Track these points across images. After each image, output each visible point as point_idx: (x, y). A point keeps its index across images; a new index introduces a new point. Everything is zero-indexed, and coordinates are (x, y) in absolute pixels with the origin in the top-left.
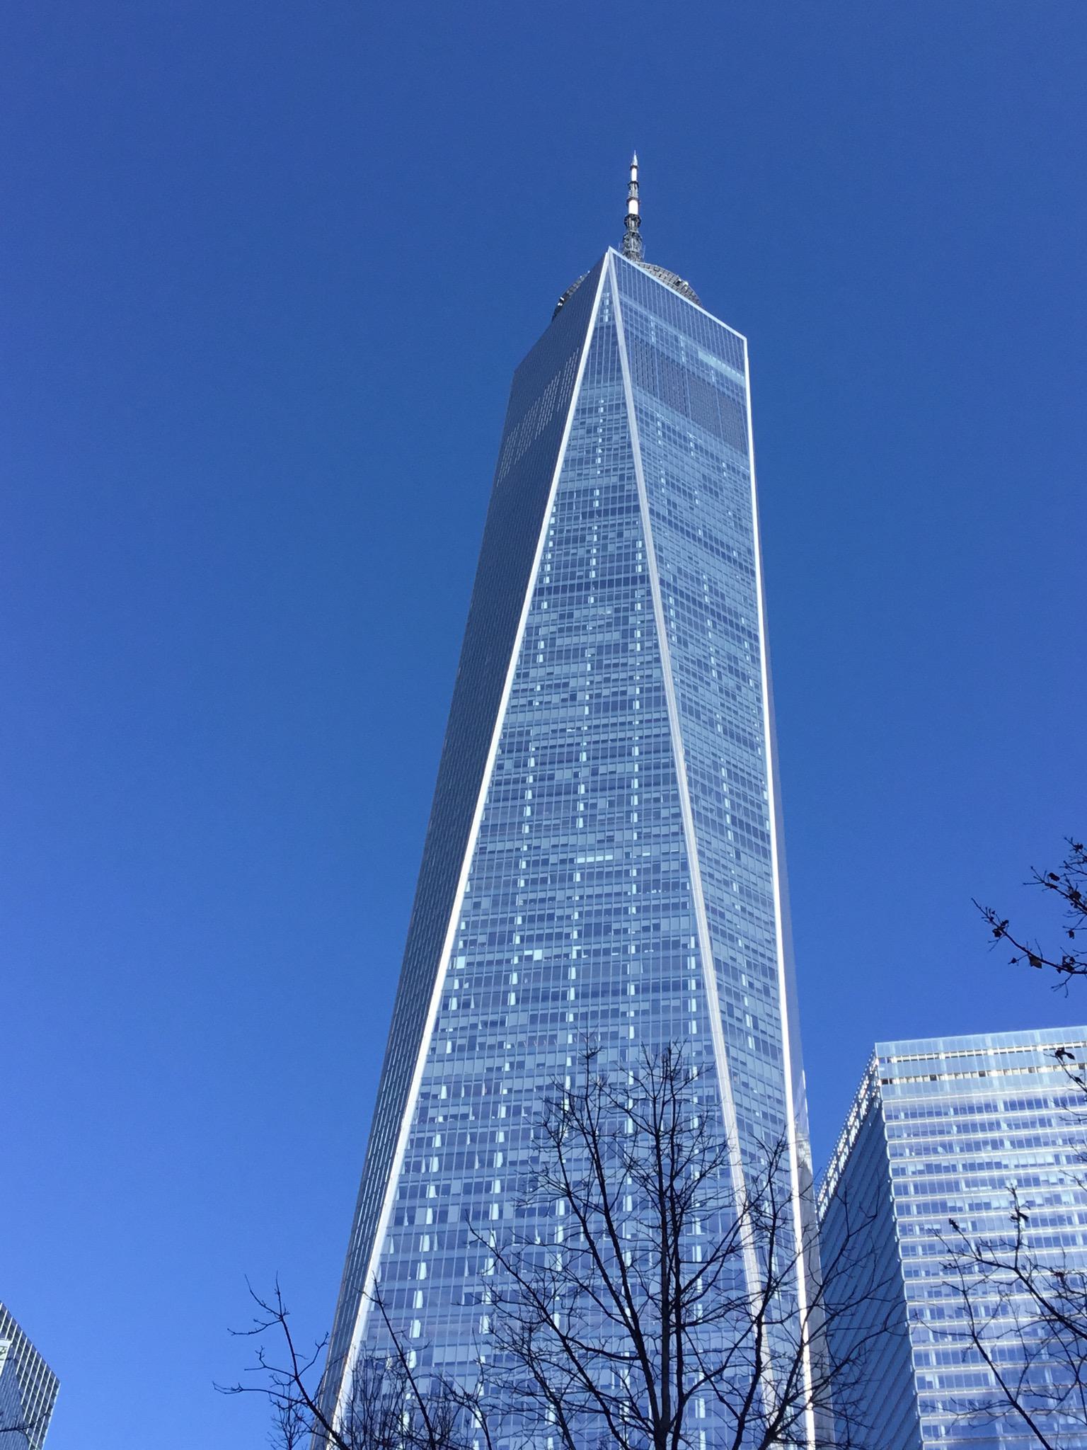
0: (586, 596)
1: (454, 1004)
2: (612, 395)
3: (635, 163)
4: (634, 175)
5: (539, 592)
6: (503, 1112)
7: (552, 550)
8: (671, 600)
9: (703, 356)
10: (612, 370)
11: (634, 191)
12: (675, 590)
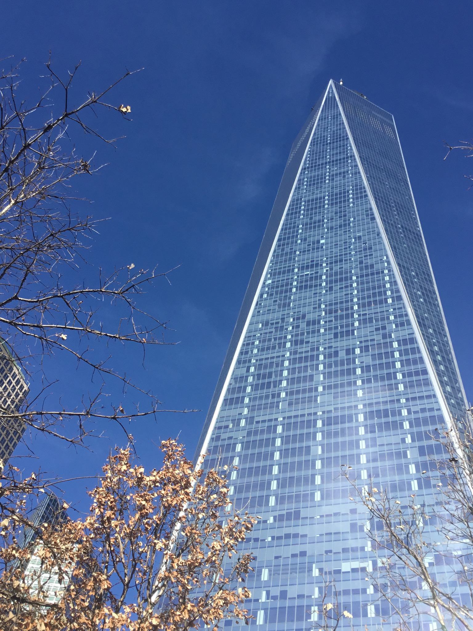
0: (325, 167)
1: (265, 296)
2: (334, 113)
4: (341, 83)
5: (304, 169)
6: (290, 328)
7: (309, 157)
10: (334, 107)
12: (367, 161)
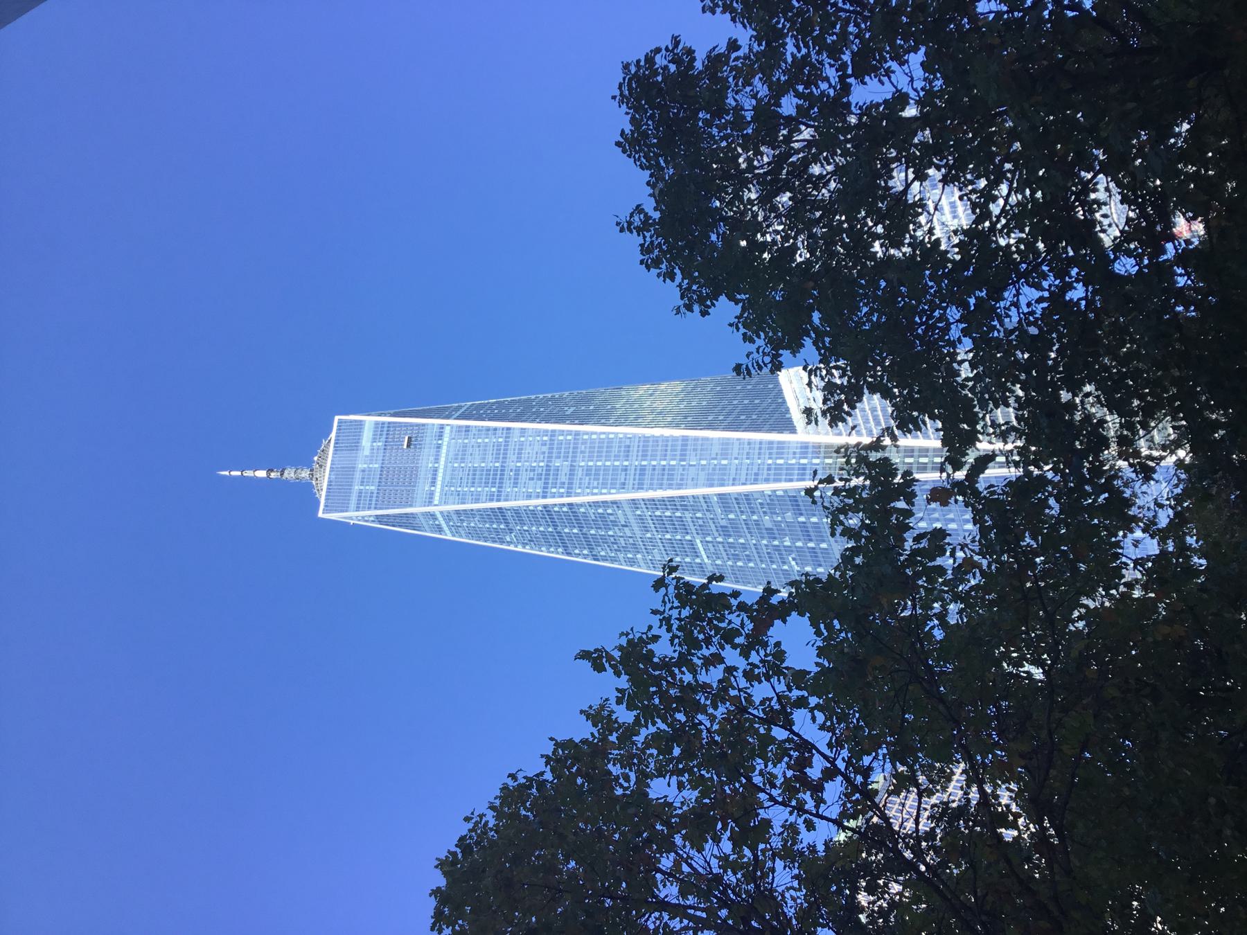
3: (227, 473)
5: (569, 554)
8: (554, 490)
9: (367, 452)
11: (249, 473)
